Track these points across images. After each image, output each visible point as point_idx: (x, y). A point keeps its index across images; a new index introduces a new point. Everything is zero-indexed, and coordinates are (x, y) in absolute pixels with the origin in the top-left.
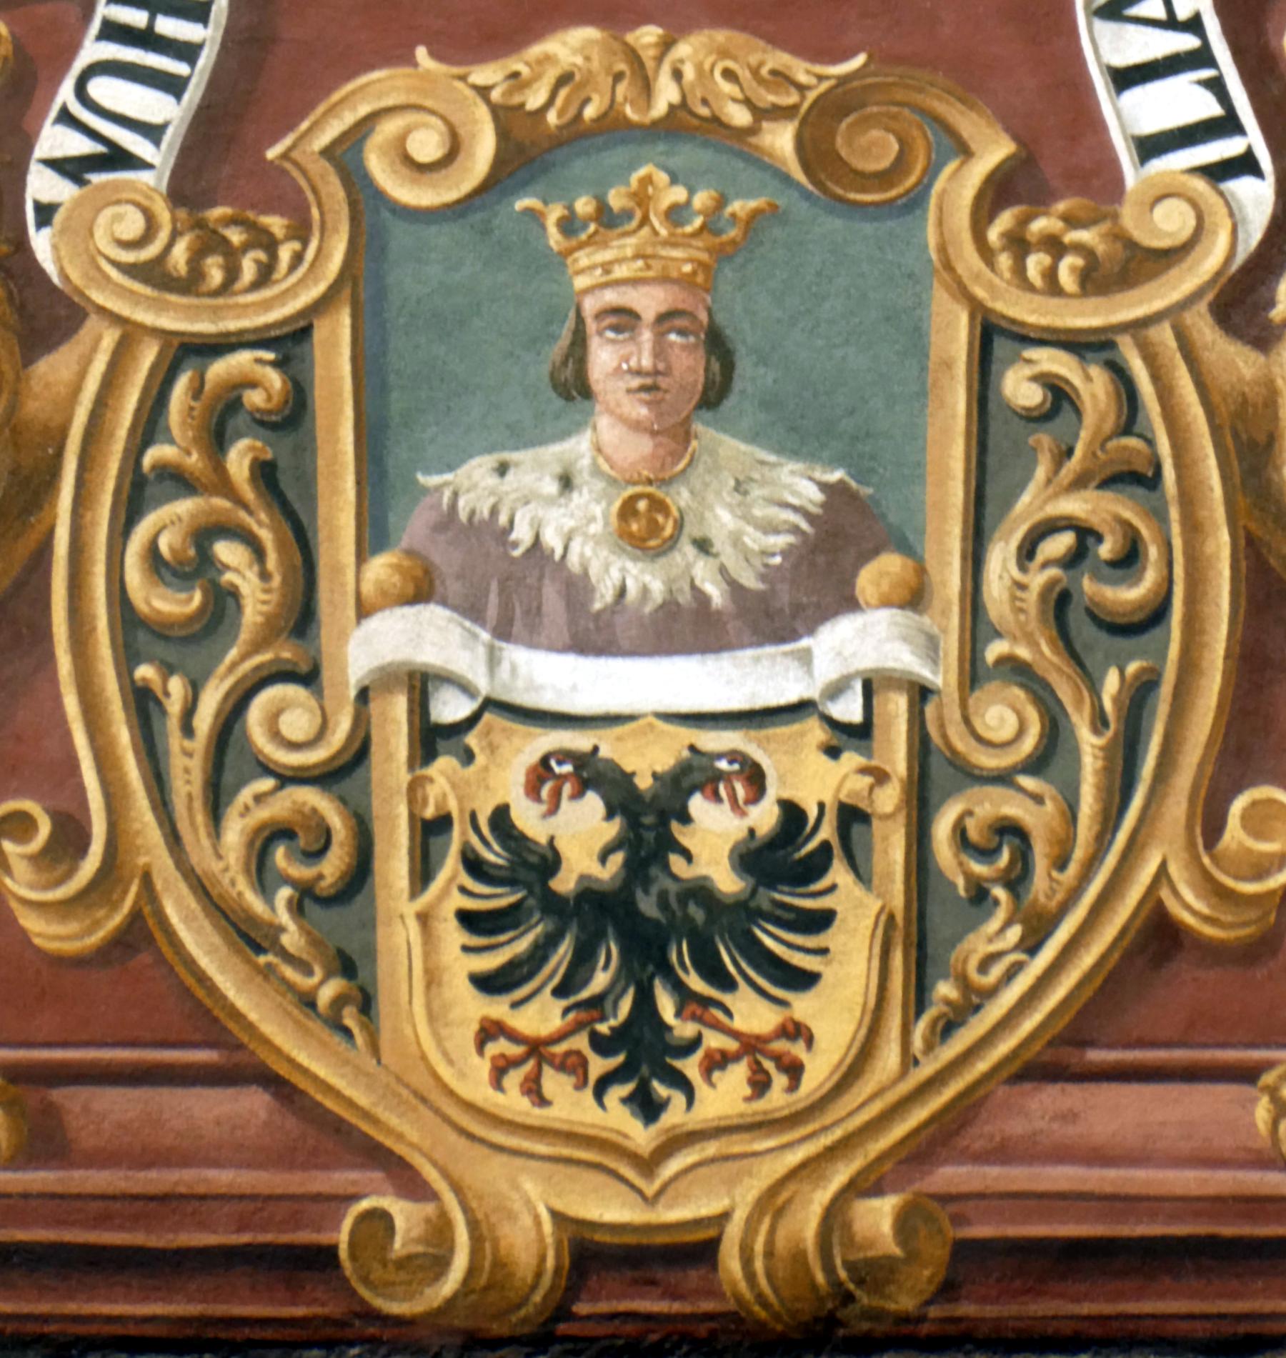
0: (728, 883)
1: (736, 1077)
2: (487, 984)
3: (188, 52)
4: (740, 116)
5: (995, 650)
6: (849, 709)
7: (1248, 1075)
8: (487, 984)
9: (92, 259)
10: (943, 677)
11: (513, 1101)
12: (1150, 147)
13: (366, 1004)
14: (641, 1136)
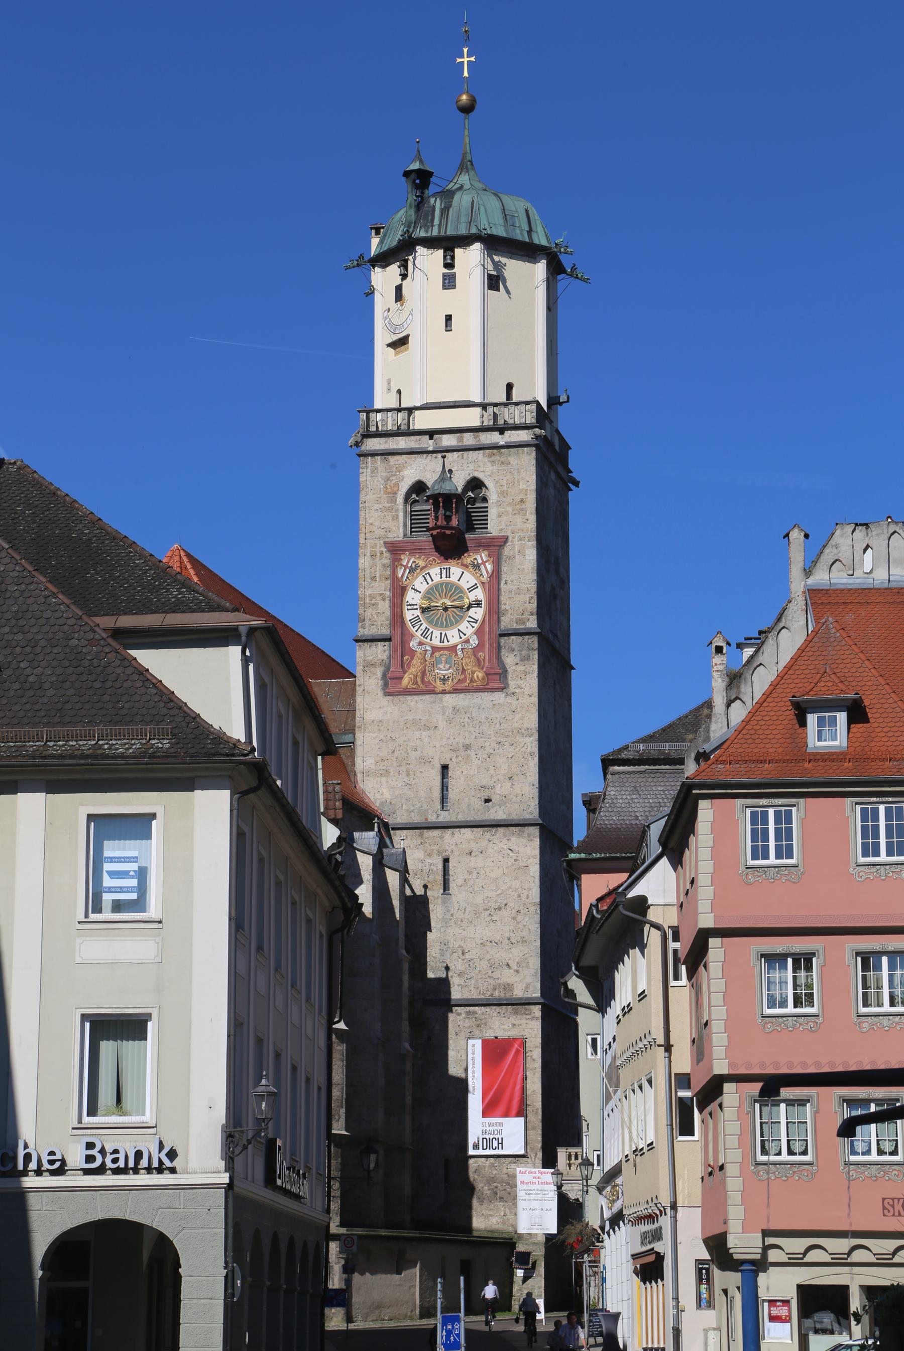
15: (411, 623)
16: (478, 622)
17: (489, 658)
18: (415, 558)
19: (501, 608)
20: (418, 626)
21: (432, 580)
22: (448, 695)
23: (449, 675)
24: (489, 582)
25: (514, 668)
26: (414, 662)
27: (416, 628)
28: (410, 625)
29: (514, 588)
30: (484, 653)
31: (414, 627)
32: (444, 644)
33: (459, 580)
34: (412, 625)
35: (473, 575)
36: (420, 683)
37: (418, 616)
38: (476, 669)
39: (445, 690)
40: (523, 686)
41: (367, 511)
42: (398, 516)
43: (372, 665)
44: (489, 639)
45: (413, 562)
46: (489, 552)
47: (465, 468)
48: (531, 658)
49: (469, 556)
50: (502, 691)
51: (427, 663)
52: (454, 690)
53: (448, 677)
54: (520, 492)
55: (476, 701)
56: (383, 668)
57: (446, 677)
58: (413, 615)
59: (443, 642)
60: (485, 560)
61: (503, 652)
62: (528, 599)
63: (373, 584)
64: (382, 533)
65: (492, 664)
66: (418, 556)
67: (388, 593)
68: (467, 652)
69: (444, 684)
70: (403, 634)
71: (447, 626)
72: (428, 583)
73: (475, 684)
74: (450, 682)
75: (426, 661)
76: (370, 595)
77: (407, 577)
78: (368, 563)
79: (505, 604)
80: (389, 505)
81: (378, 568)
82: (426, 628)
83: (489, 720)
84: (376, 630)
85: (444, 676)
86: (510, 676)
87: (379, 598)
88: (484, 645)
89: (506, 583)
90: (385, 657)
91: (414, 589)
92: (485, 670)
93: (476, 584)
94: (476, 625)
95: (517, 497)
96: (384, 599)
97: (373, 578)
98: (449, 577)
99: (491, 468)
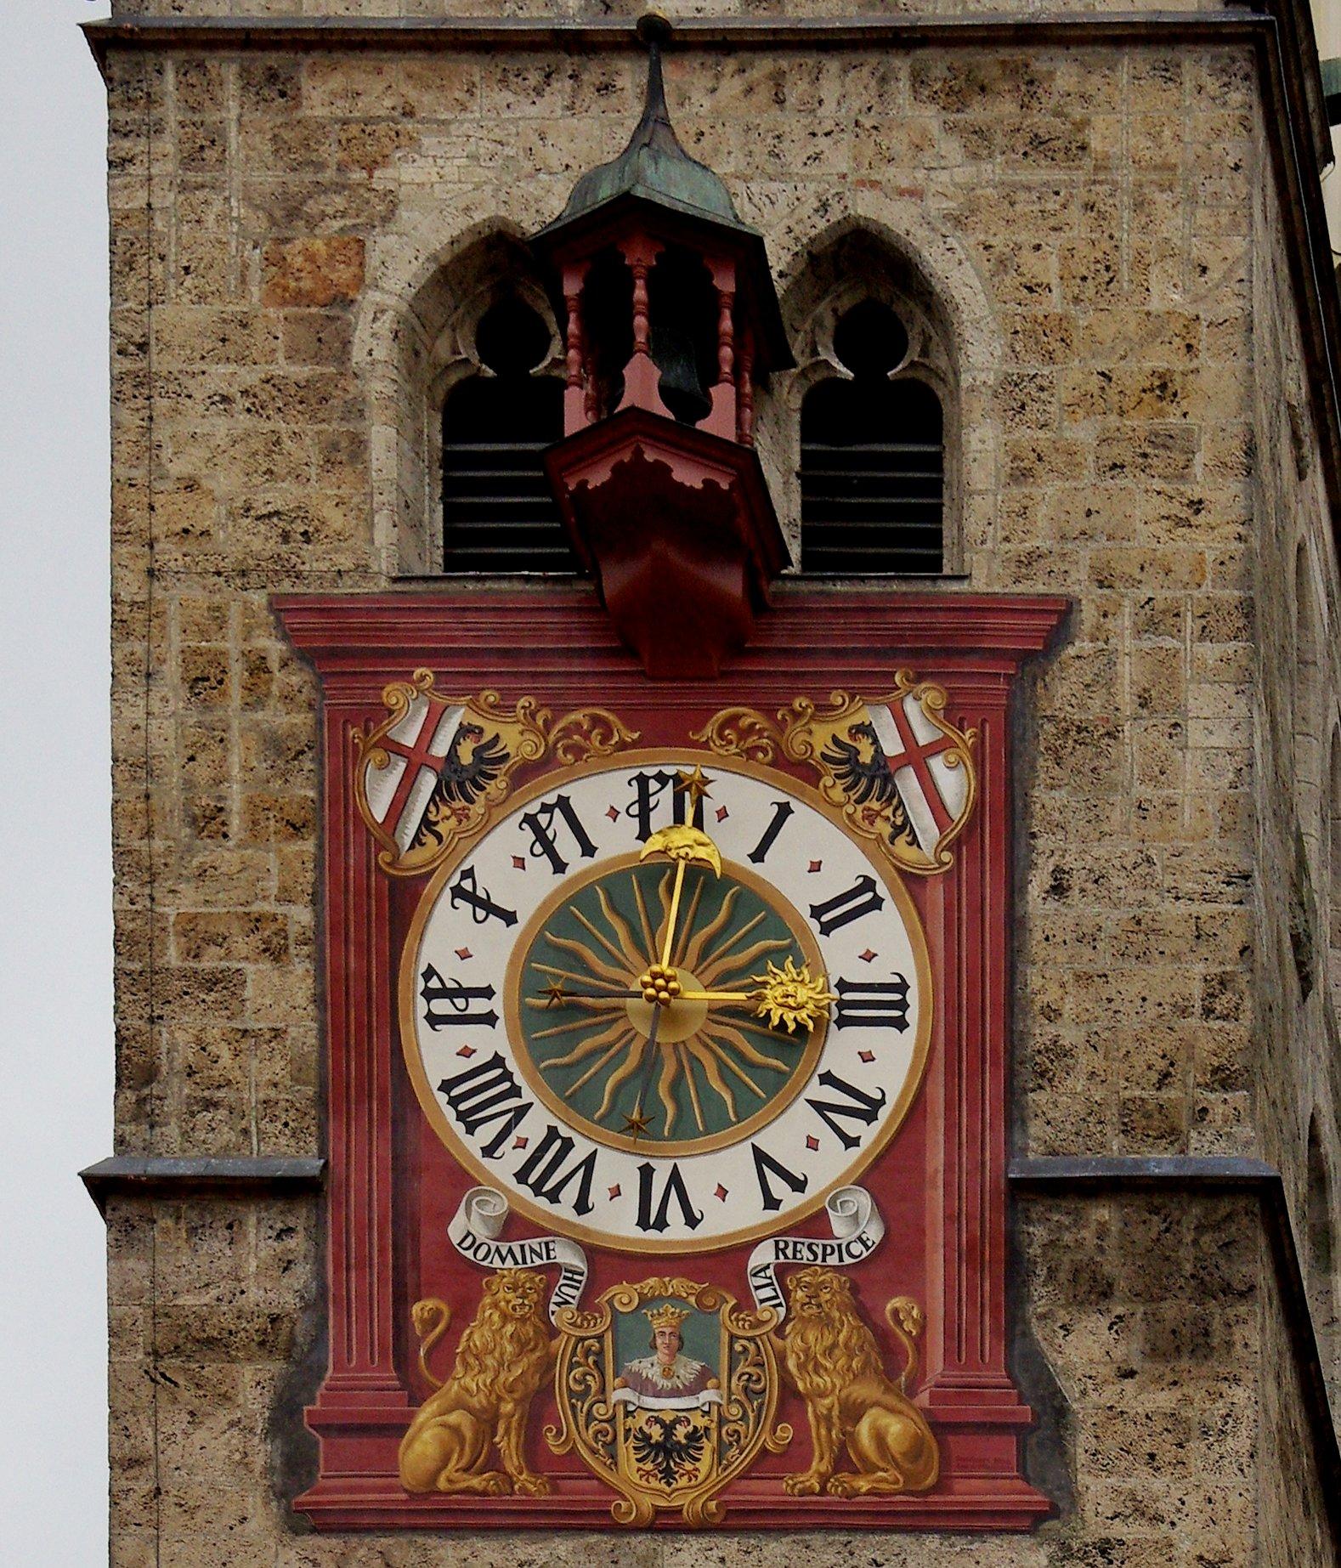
0: (684, 1441)
1: (685, 1478)
2: (639, 1460)
3: (580, 1282)
4: (685, 1295)
5: (733, 1397)
6: (706, 1408)
7: (782, 1478)
8: (639, 1460)
9: (562, 1321)
10: (723, 1402)
11: (643, 1483)
12: (762, 1301)
13: (616, 1465)
14: (668, 1490)
15: (454, 1102)
16: (884, 1113)
17: (953, 1334)
18: (474, 706)
19: (1025, 1035)
20: (500, 1123)
21: (588, 849)
23: (699, 1421)
24: (951, 877)
25: (1109, 1395)
26: (476, 1335)
27: (487, 1133)
28: (450, 1114)
29: (1113, 919)
31: (471, 1129)
32: (668, 1234)
33: (758, 856)
34: (461, 1116)
35: (850, 827)
36: (512, 1463)
37: (498, 1061)
38: (865, 1391)
39: (678, 1511)
40: (1164, 1507)
41: (162, 404)
42: (359, 445)
43: (210, 1342)
45: (465, 731)
46: (952, 693)
47: (797, 168)
48: (1215, 1341)
49: (824, 710)
50: (1030, 1532)
51: (559, 1344)
53: (693, 1436)
54: (1154, 335)
56: (276, 1367)
57: (681, 1432)
58: (466, 1053)
59: (661, 1224)
60: (924, 736)
61: (1041, 1296)
62: (1197, 989)
63: (207, 853)
64: (257, 544)
66: (493, 697)
67: (301, 916)
69: (668, 1475)
70: (402, 1168)
71: (683, 1130)
72: (559, 866)
73: (863, 1485)
74: (704, 1465)
75: (554, 1333)
76: (189, 925)
77: (426, 823)
78: (169, 727)
79: (1052, 1013)
80: (301, 372)
81: (235, 760)
82: (553, 1133)
84: (227, 1136)
86: (1082, 1444)
87: (242, 945)
88: (918, 1253)
89: (1058, 889)
90: (290, 1301)
91: (472, 898)
92: (923, 1399)
93: (868, 884)
95: (1132, 364)
96: (275, 953)
97: (209, 822)
99: (964, 174)
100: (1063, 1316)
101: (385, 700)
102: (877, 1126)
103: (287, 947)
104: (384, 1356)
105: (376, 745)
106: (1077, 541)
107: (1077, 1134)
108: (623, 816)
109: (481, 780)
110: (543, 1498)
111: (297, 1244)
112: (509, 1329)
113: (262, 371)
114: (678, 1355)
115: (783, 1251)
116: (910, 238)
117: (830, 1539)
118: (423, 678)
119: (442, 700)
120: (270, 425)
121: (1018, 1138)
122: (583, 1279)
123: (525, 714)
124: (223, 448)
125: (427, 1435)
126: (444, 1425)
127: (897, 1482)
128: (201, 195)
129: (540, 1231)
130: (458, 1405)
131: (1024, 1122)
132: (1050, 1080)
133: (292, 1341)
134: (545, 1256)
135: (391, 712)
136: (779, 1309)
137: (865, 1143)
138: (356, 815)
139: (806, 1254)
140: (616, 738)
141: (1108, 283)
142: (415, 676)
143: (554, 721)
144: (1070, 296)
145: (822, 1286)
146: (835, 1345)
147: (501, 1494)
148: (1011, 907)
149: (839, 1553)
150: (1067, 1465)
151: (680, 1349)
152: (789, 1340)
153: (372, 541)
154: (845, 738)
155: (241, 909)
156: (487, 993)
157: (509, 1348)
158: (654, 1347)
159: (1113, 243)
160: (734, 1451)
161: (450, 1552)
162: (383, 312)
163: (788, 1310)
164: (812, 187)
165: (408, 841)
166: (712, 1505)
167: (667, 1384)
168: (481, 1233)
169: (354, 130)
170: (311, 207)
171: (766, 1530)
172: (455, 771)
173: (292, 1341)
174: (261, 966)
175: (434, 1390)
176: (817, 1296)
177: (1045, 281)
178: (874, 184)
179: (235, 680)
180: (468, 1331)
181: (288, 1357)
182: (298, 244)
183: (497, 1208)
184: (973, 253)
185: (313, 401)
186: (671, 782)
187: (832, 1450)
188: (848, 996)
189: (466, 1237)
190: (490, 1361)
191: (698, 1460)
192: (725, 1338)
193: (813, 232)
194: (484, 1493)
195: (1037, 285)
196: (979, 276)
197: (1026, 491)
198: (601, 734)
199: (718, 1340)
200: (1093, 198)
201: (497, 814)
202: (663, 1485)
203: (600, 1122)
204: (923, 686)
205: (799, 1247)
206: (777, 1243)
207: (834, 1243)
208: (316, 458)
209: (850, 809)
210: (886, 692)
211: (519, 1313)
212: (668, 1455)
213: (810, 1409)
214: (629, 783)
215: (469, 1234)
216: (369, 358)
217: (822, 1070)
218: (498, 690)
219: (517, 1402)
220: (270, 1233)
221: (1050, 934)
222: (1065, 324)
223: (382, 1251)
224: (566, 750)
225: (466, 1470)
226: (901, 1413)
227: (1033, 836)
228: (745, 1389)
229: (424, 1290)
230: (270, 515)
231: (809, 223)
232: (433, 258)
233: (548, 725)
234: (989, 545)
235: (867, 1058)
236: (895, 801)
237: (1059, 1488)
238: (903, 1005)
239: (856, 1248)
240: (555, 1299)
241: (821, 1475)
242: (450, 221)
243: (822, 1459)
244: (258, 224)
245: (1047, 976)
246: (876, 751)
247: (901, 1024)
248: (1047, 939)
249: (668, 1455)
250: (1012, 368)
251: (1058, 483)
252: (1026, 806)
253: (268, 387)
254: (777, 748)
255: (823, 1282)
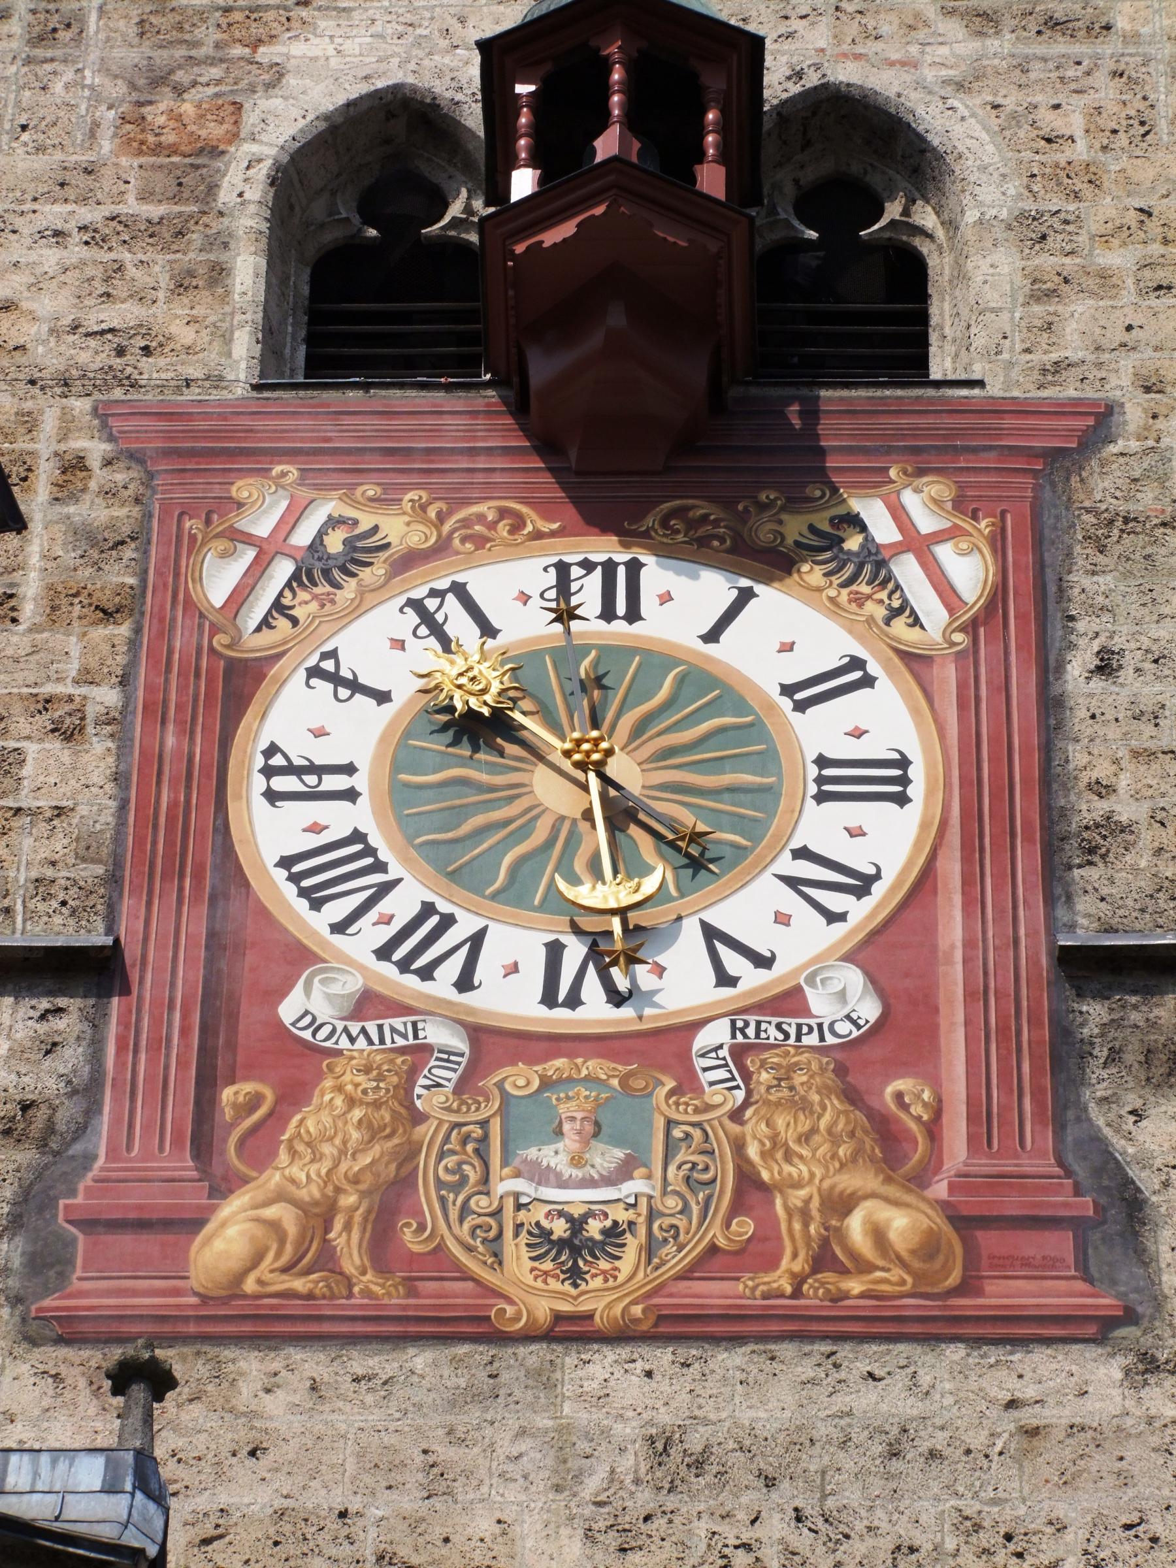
0: (598, 1237)
1: (600, 1279)
2: (532, 1259)
3: (459, 1064)
4: (604, 1077)
5: (669, 1189)
6: (632, 1200)
7: (738, 1279)
8: (532, 1259)
9: (432, 1106)
10: (656, 1194)
12: (712, 1084)
13: (500, 1263)
14: (573, 1292)
15: (295, 878)
16: (878, 889)
22: (610, 1354)
27: (337, 910)
28: (290, 890)
30: (935, 1083)
31: (316, 905)
32: (580, 1013)
33: (712, 636)
34: (303, 893)
35: (834, 608)
39: (589, 1316)
42: (219, 273)
44: (975, 995)
46: (961, 486)
51: (425, 1131)
52: (661, 1319)
53: (614, 1232)
55: (864, 1399)
57: (594, 1228)
58: (316, 828)
59: (574, 1000)
60: (926, 522)
64: (84, 357)
65: (999, 1155)
67: (107, 696)
68: (784, 1076)
69: (575, 1275)
75: (418, 1118)
77: (278, 606)
80: (155, 211)
83: (984, 1539)
85: (577, 1224)
89: (1106, 666)
90: (52, 1086)
91: (335, 679)
92: (940, 1189)
94: (859, 910)
98: (633, 615)
100: (1132, 1100)
101: (234, 494)
102: (869, 902)
103: (82, 729)
104: (177, 1141)
105: (217, 536)
106: (1116, 353)
107: (1143, 911)
108: (536, 602)
109: (353, 568)
110: (394, 1301)
111: (68, 1024)
112: (357, 1113)
113: (108, 210)
114: (593, 1143)
115: (742, 1031)
116: (902, 99)
117: (807, 1348)
118: (284, 474)
119: (305, 494)
120: (113, 255)
121: (1061, 913)
122: (464, 1060)
123: (413, 507)
124: (51, 274)
125: (232, 1231)
126: (258, 1220)
127: (903, 1282)
128: (48, 67)
129: (405, 1010)
130: (280, 1197)
131: (1069, 898)
132: (1103, 857)
133: (50, 1128)
134: (411, 1036)
135: (240, 505)
136: (736, 1092)
137: (853, 920)
138: (189, 603)
139: (773, 1033)
140: (529, 528)
141: (1144, 135)
142: (274, 473)
143: (450, 513)
144: (1098, 146)
145: (793, 1068)
146: (814, 1130)
147: (333, 1297)
148: (1044, 685)
149: (819, 1365)
150: (1146, 1265)
151: (596, 1135)
152: (748, 1128)
153: (229, 355)
154: (826, 527)
155: (25, 690)
156: (349, 769)
157: (355, 1135)
158: (559, 1133)
159: (1147, 103)
160: (670, 1248)
161: (255, 1365)
162: (260, 161)
163: (749, 1093)
164: (784, 59)
165: (253, 624)
166: (637, 1310)
167: (577, 1173)
168: (324, 1011)
169: (238, 16)
170: (180, 76)
171: (715, 1340)
172: (320, 559)
173: (50, 1128)
174: (47, 746)
175: (245, 1181)
176: (788, 1078)
177: (1068, 133)
178: (858, 57)
179: (43, 478)
180: (298, 1117)
181: (42, 1144)
182: (162, 106)
183: (347, 986)
184: (980, 112)
185: (167, 236)
186: (599, 568)
187: (808, 1245)
188: (829, 772)
189: (302, 1017)
190: (327, 1149)
191: (619, 1258)
192: (660, 1123)
193: (785, 96)
194: (310, 1296)
195: (1057, 137)
196: (986, 128)
197: (1051, 309)
198: (511, 525)
199: (650, 1123)
200: (1122, 67)
201: (370, 599)
202: (567, 1287)
203: (494, 897)
204: (925, 479)
205: (764, 1026)
206: (733, 1022)
207: (813, 1022)
208: (165, 281)
209: (832, 593)
210: (877, 485)
211: (371, 1097)
212: (576, 1252)
213: (778, 1202)
214: (545, 569)
215: (307, 1013)
216: (239, 200)
217: (796, 844)
218: (378, 484)
219: (363, 1194)
220: (32, 1013)
221: (1098, 712)
222: (1093, 169)
223: (185, 1032)
224: (464, 540)
225: (285, 1270)
226: (907, 1205)
227: (1072, 618)
228: (688, 1179)
229: (239, 1073)
230: (103, 333)
231: (781, 88)
232: (326, 117)
233: (441, 518)
234: (1005, 356)
235: (855, 833)
236: (891, 586)
237: (1137, 1290)
238: (904, 781)
239: (844, 1028)
240: (422, 1081)
241: (793, 1275)
242: (348, 87)
243: (795, 1255)
244: (118, 89)
245: (1096, 752)
246: (866, 539)
247: (902, 800)
248: (1093, 717)
249: (576, 1252)
250: (1030, 206)
251: (1092, 302)
252: (1061, 590)
253: (114, 224)
254: (738, 538)
255: (796, 1064)
